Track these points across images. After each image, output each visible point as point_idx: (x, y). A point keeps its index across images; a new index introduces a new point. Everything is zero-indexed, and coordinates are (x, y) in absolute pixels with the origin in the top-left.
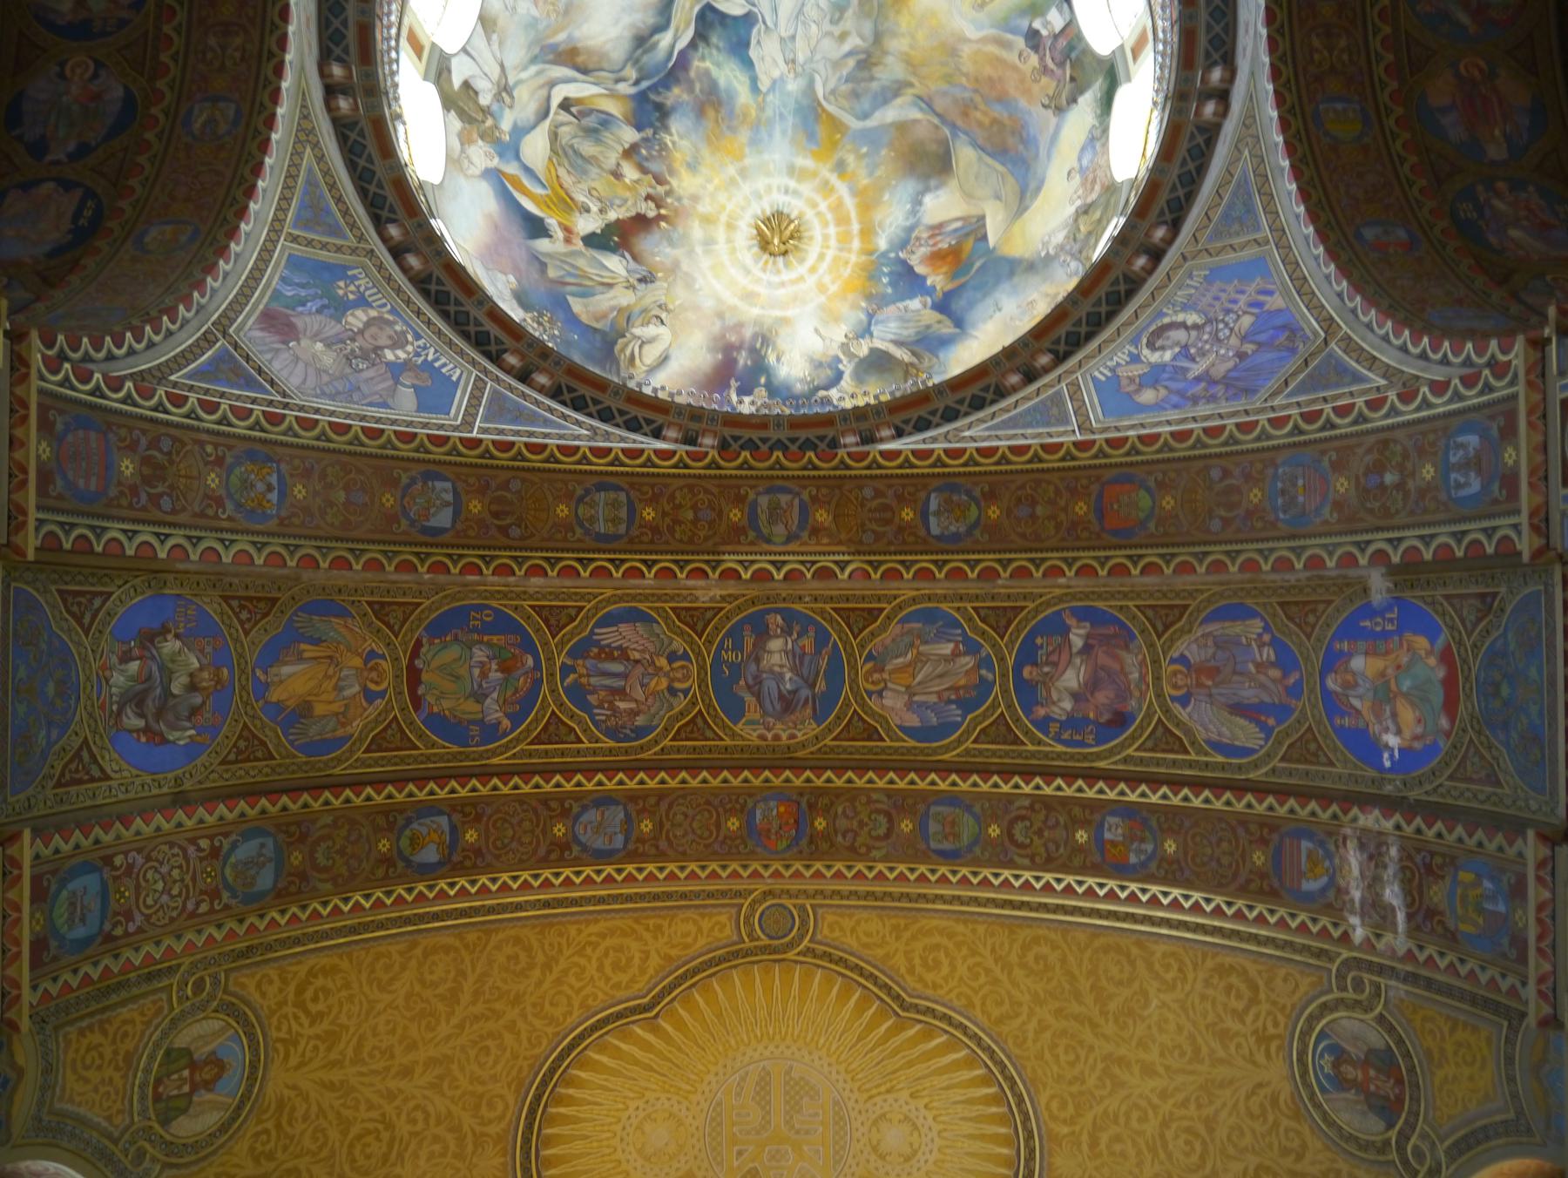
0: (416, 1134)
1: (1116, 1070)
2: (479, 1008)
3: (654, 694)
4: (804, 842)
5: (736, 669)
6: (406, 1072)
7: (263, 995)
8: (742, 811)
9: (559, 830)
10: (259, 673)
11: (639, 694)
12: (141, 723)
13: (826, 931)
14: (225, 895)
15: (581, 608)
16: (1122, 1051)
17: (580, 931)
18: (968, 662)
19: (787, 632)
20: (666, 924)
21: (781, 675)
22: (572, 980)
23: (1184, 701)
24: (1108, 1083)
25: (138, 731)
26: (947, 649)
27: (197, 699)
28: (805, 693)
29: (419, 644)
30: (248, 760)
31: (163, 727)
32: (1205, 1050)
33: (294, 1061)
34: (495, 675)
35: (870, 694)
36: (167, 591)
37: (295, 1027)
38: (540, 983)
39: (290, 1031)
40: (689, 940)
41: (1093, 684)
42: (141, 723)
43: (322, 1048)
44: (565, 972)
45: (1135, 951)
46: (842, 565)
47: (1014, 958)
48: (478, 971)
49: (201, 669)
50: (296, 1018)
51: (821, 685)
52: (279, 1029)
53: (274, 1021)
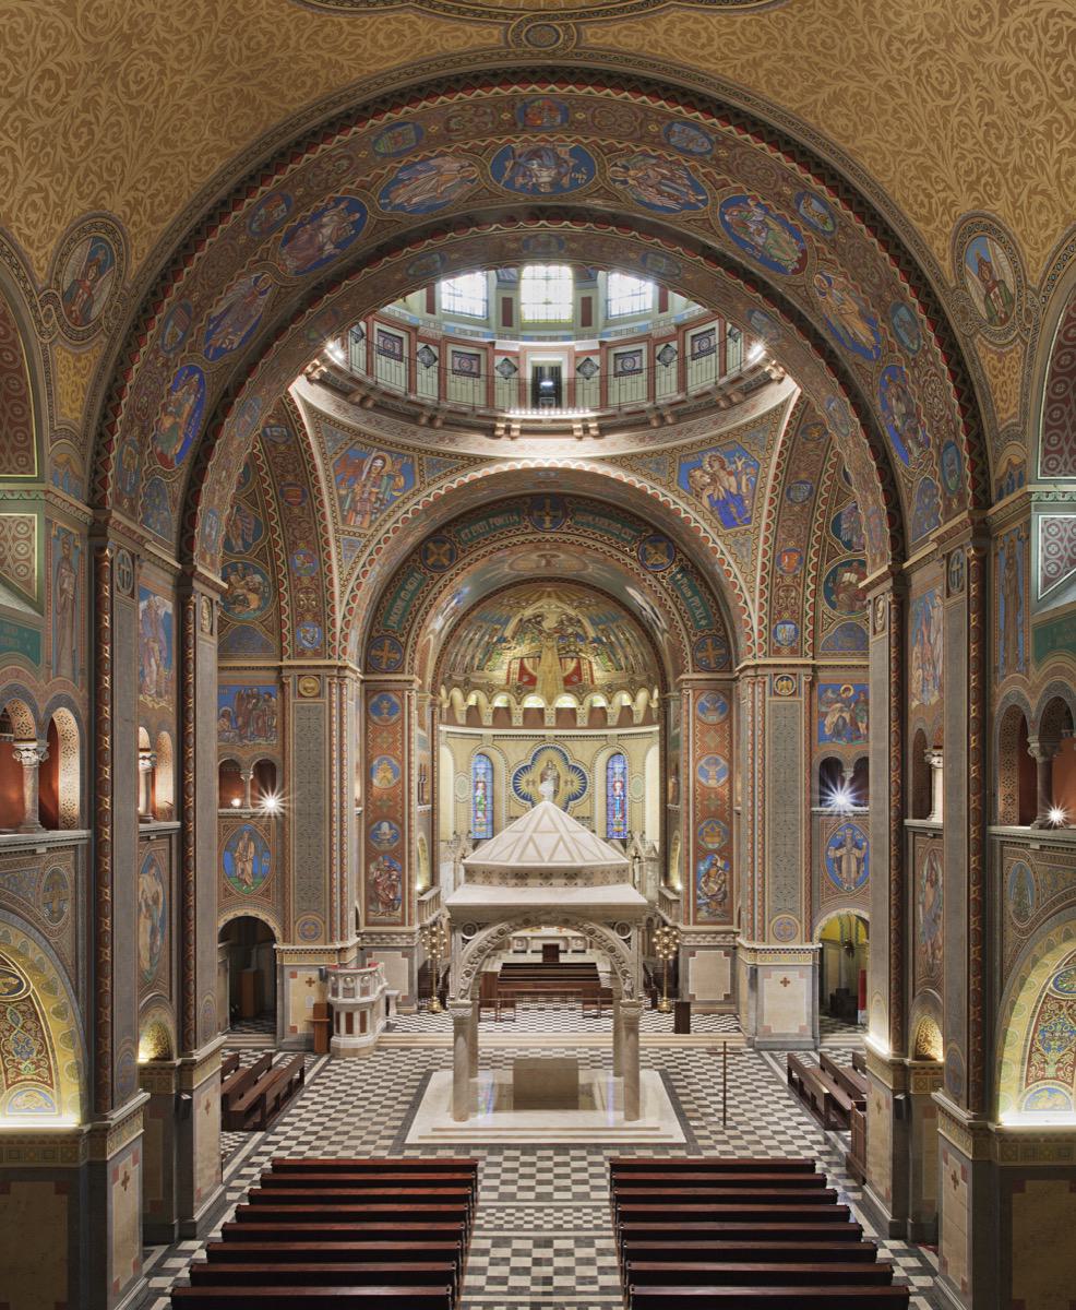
0: (902, 41)
1: (213, 66)
2: (821, 76)
3: (640, 169)
4: (519, 105)
5: (576, 169)
6: (889, 88)
8: (572, 122)
9: (723, 153)
11: (651, 173)
13: (496, 32)
15: (688, 222)
16: (214, 84)
17: (724, 69)
18: (398, 201)
19: (536, 186)
20: (646, 48)
21: (539, 165)
22: (738, 46)
23: (257, 279)
24: (217, 52)
26: (414, 200)
28: (522, 160)
29: (795, 271)
32: (163, 150)
34: (753, 228)
35: (471, 165)
38: (767, 57)
40: (625, 32)
41: (312, 238)
44: (741, 51)
45: (234, 147)
46: (497, 229)
47: (323, 73)
48: (814, 97)
51: (509, 164)
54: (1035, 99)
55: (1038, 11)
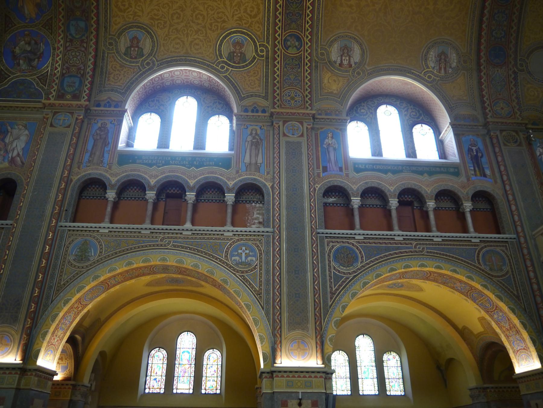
7: (119, 23)
10: (27, 21)
12: (37, 60)
14: (84, 38)
25: (38, 61)
27: (33, 42)
30: (52, 26)
31: (39, 53)
33: (140, 14)
36: (2, 51)
37: (131, 13)
39: (132, 15)
42: (37, 60)
43: (139, 4)
49: (25, 40)
50: (129, 12)
52: (130, 18)
53: (127, 19)
54: (200, 22)
55: (220, 8)
